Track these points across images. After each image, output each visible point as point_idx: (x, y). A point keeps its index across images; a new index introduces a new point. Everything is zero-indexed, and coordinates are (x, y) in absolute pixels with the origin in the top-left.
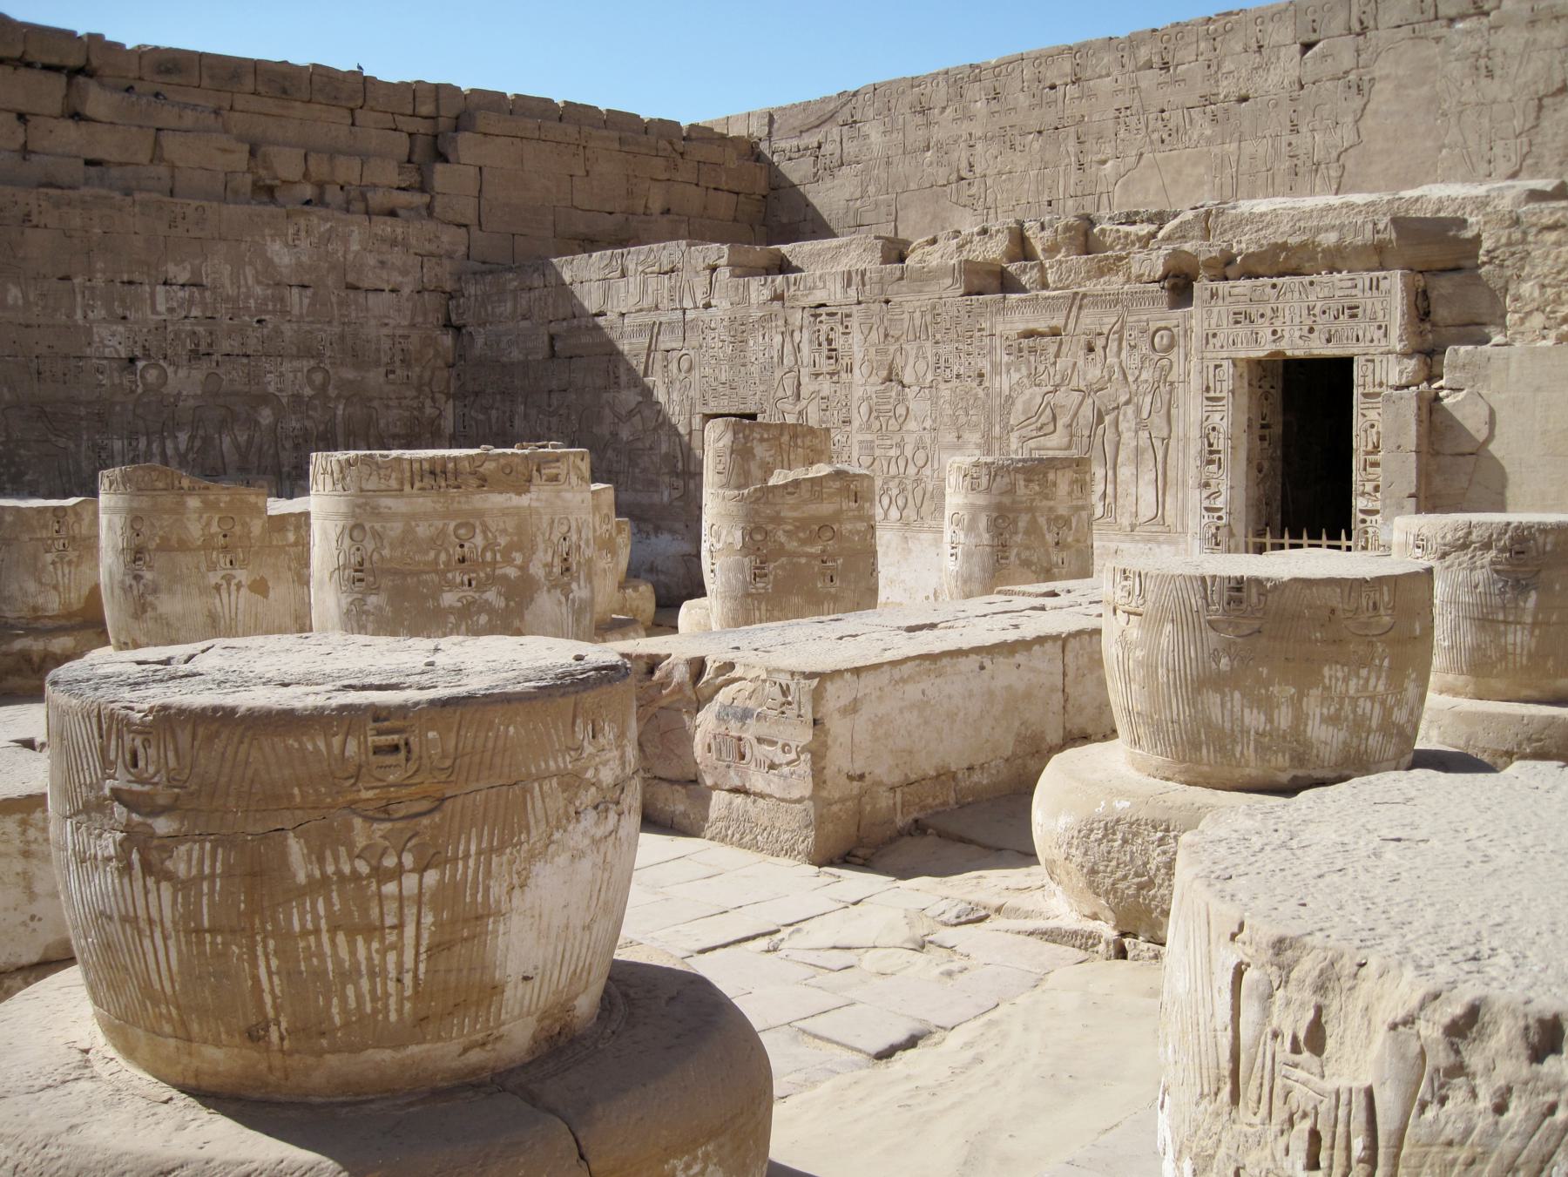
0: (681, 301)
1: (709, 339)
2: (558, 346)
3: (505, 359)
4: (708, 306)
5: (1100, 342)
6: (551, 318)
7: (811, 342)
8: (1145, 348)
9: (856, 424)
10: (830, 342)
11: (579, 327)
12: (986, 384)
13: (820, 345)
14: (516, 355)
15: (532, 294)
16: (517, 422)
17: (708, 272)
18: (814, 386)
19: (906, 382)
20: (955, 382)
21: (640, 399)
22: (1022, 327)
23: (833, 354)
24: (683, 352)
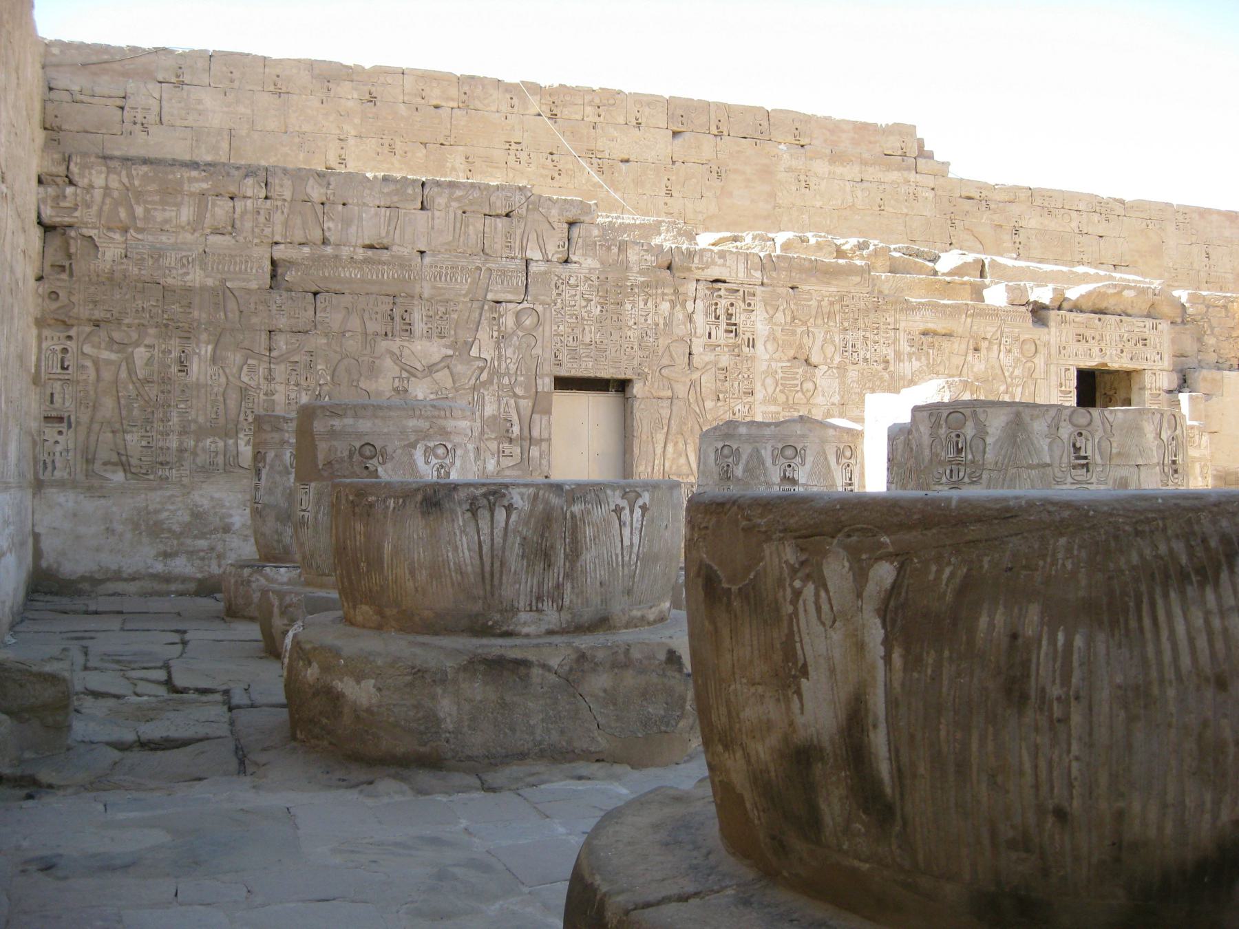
0: (523, 249)
1: (566, 296)
2: (290, 276)
3: (170, 281)
4: (566, 261)
5: (984, 344)
6: (277, 238)
7: (706, 314)
8: (1016, 351)
9: (759, 395)
10: (730, 316)
11: (336, 257)
12: (891, 368)
13: (717, 318)
14: (196, 277)
15: (239, 204)
16: (194, 367)
17: (566, 226)
18: (710, 357)
19: (814, 359)
20: (862, 365)
21: (450, 352)
22: (922, 327)
23: (733, 329)
24: (525, 305)
